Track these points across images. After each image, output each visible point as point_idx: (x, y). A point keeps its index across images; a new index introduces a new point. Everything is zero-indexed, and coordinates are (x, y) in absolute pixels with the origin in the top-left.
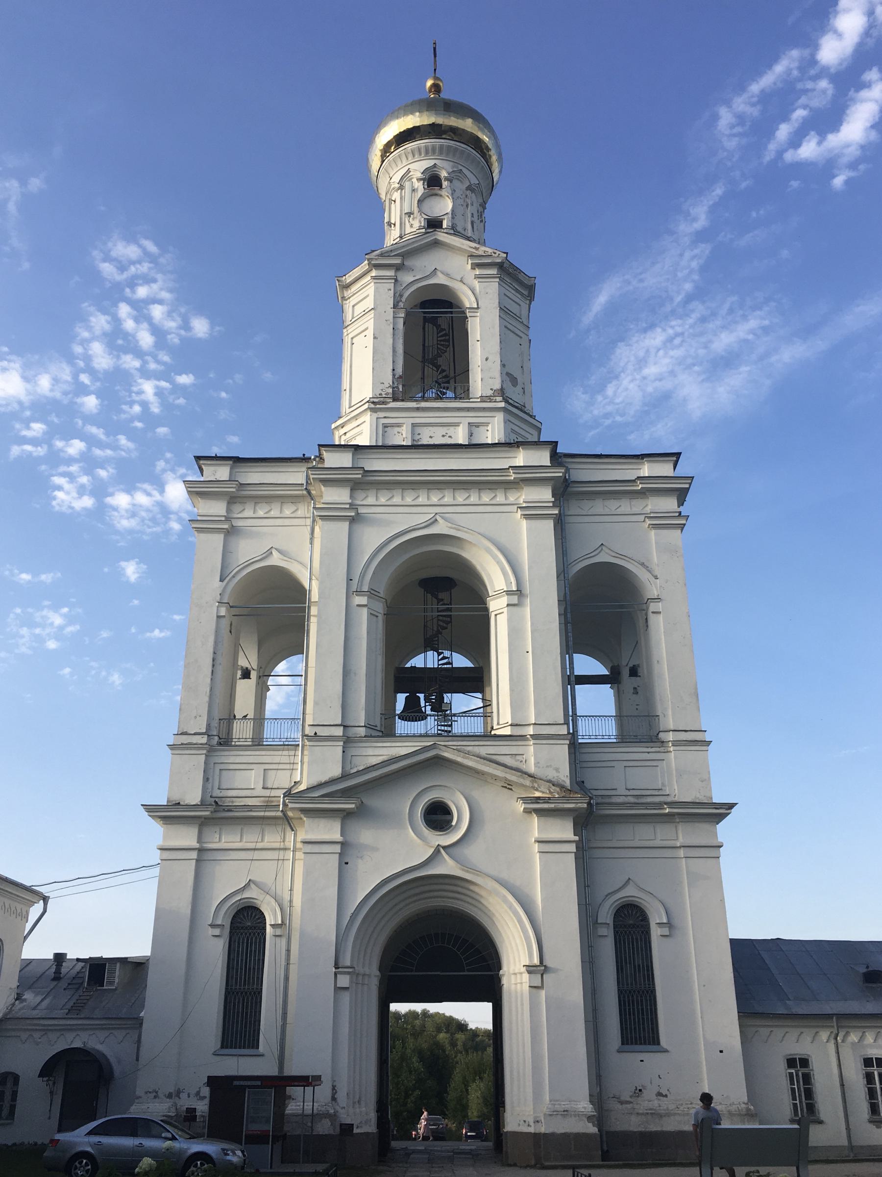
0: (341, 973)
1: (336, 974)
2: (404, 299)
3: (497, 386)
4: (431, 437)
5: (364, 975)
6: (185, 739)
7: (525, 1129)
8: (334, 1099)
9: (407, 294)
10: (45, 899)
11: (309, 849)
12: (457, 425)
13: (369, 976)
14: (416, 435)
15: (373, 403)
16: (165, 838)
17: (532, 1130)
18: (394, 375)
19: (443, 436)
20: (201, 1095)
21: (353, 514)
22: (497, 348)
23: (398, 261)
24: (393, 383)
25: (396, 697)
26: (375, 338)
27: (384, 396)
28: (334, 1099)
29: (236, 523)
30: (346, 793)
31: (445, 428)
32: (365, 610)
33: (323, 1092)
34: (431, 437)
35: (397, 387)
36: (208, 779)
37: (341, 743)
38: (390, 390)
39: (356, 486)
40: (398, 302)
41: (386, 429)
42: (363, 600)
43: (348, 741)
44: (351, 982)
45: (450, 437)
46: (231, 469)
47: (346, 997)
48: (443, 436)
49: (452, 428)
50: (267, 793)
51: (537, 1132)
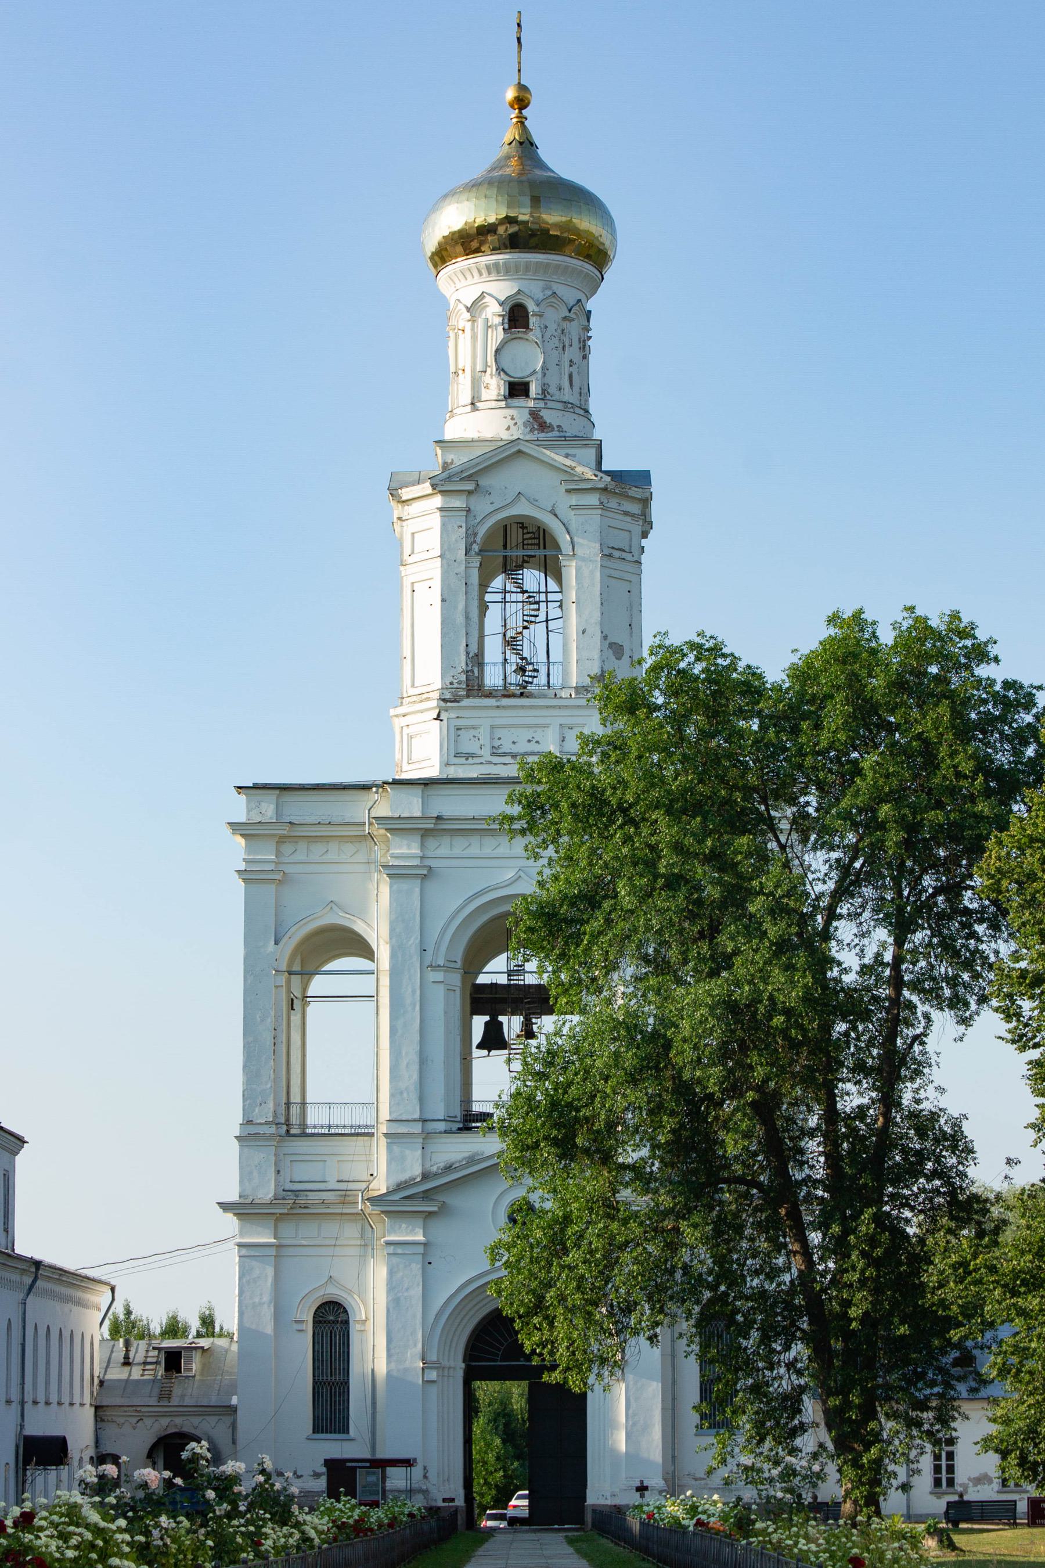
0: (427, 1368)
1: (423, 1369)
2: (478, 539)
3: (596, 670)
4: (514, 743)
5: (449, 1368)
6: (252, 1129)
7: (602, 1502)
8: (425, 1477)
9: (482, 531)
10: (113, 1290)
11: (391, 1250)
12: (546, 726)
13: (454, 1368)
14: (496, 740)
15: (444, 700)
16: (242, 1234)
17: (608, 1502)
18: (468, 653)
19: (529, 741)
20: (299, 1474)
21: (425, 872)
22: (597, 615)
23: (470, 486)
24: (467, 664)
25: (472, 1018)
26: (443, 600)
27: (456, 685)
28: (425, 1477)
29: (288, 869)
30: (426, 1196)
31: (532, 730)
32: (442, 985)
33: (417, 1471)
34: (514, 743)
35: (472, 671)
36: (278, 1172)
37: (421, 1140)
38: (463, 677)
39: (426, 834)
40: (471, 545)
41: (459, 732)
42: (439, 976)
43: (427, 1136)
44: (438, 1376)
45: (537, 742)
46: (278, 798)
47: (433, 1390)
48: (529, 741)
49: (539, 730)
50: (343, 1186)
51: (613, 1503)
